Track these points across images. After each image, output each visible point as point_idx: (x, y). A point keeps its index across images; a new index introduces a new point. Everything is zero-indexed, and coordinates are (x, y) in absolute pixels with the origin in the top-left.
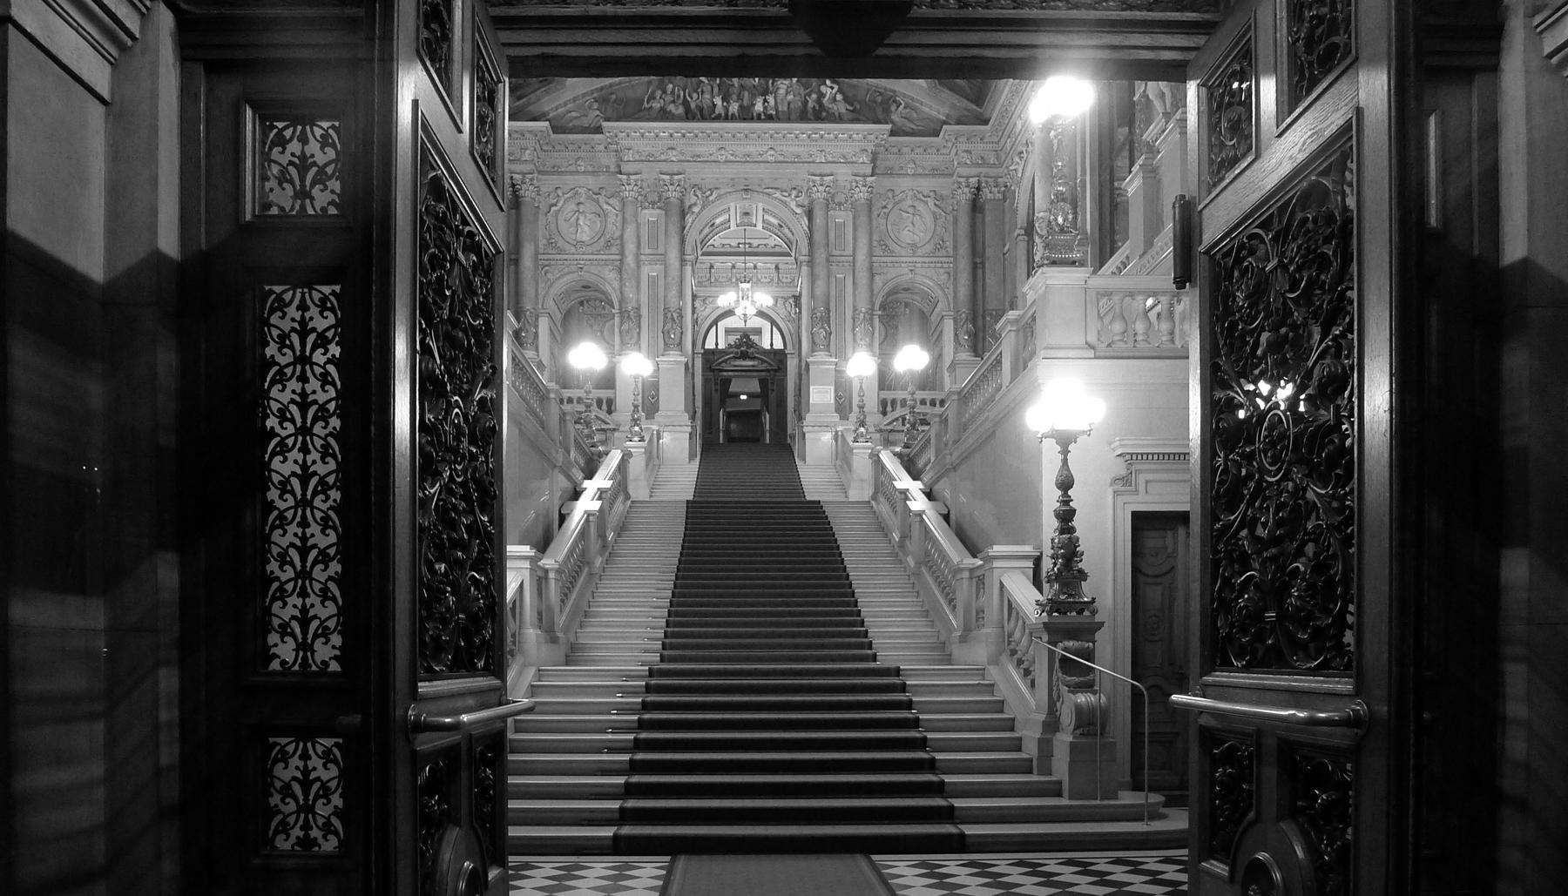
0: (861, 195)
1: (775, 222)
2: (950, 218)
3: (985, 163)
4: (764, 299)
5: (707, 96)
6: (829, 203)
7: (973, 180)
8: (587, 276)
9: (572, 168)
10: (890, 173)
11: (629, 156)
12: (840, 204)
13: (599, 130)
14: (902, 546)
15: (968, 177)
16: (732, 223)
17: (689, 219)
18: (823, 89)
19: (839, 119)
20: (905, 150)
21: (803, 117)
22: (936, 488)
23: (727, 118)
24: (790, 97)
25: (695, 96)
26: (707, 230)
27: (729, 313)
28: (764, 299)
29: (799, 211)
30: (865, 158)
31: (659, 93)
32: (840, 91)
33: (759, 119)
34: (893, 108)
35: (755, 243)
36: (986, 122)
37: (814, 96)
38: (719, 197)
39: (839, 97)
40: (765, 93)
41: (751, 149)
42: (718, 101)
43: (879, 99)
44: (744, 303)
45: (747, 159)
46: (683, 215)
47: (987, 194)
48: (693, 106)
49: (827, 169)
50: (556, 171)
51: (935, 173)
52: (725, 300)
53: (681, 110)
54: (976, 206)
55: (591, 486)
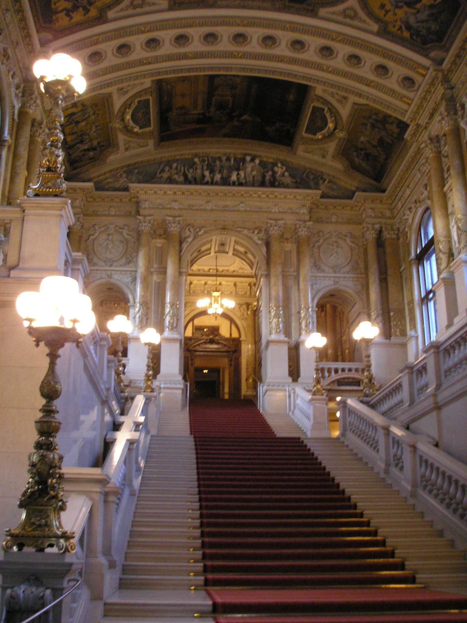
0: (303, 232)
1: (242, 250)
2: (362, 250)
3: (383, 216)
4: (230, 304)
5: (199, 171)
6: (282, 238)
7: (377, 226)
8: (112, 281)
9: (106, 213)
10: (319, 221)
11: (146, 205)
12: (287, 239)
13: (126, 189)
14: (387, 472)
15: (373, 224)
16: (212, 250)
17: (185, 246)
18: (276, 169)
19: (287, 186)
20: (330, 207)
21: (263, 184)
22: (412, 426)
23: (212, 183)
24: (254, 173)
25: (191, 171)
26: (195, 255)
27: (204, 313)
28: (230, 304)
29: (260, 242)
30: (304, 210)
31: (167, 168)
32: (286, 170)
33: (234, 184)
34: (321, 182)
35: (220, 269)
36: (384, 191)
37: (270, 173)
38: (205, 232)
39: (286, 174)
40: (238, 169)
41: (228, 203)
42: (207, 173)
43: (312, 177)
44: (215, 305)
45: (225, 209)
46: (181, 243)
47: (386, 235)
48: (190, 176)
49: (280, 216)
50: (95, 214)
51: (349, 222)
52: (202, 303)
53: (182, 179)
54: (380, 243)
55: (128, 421)
